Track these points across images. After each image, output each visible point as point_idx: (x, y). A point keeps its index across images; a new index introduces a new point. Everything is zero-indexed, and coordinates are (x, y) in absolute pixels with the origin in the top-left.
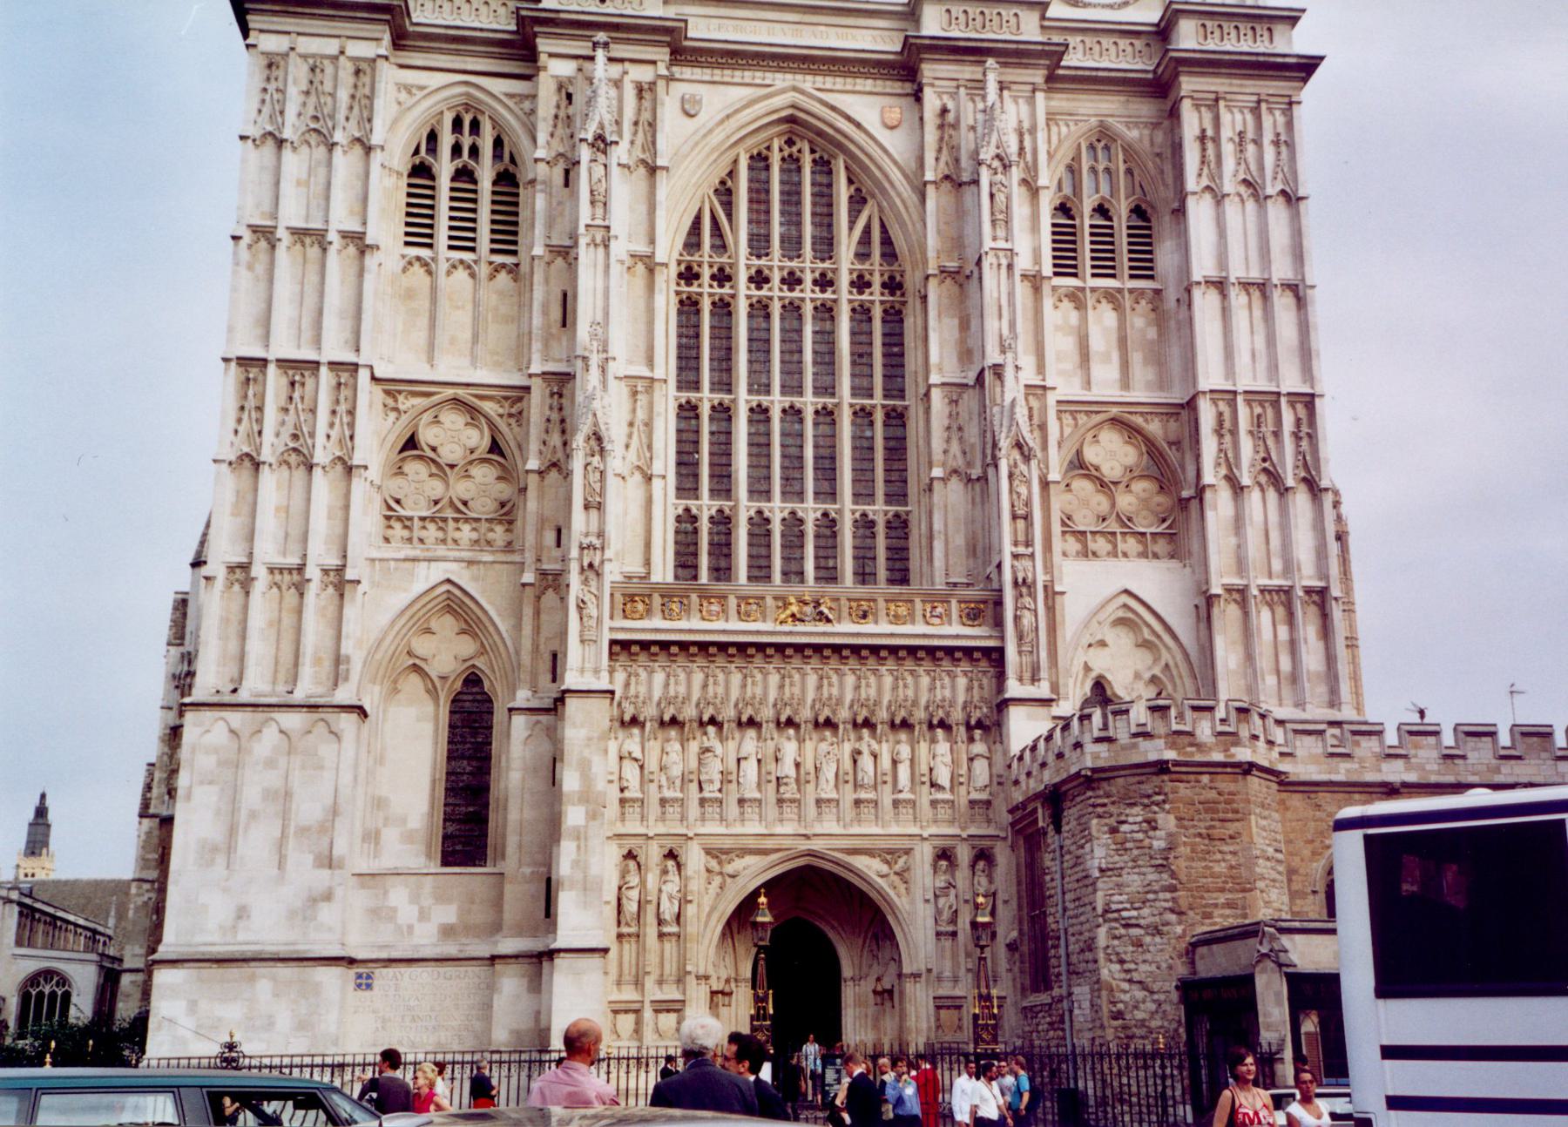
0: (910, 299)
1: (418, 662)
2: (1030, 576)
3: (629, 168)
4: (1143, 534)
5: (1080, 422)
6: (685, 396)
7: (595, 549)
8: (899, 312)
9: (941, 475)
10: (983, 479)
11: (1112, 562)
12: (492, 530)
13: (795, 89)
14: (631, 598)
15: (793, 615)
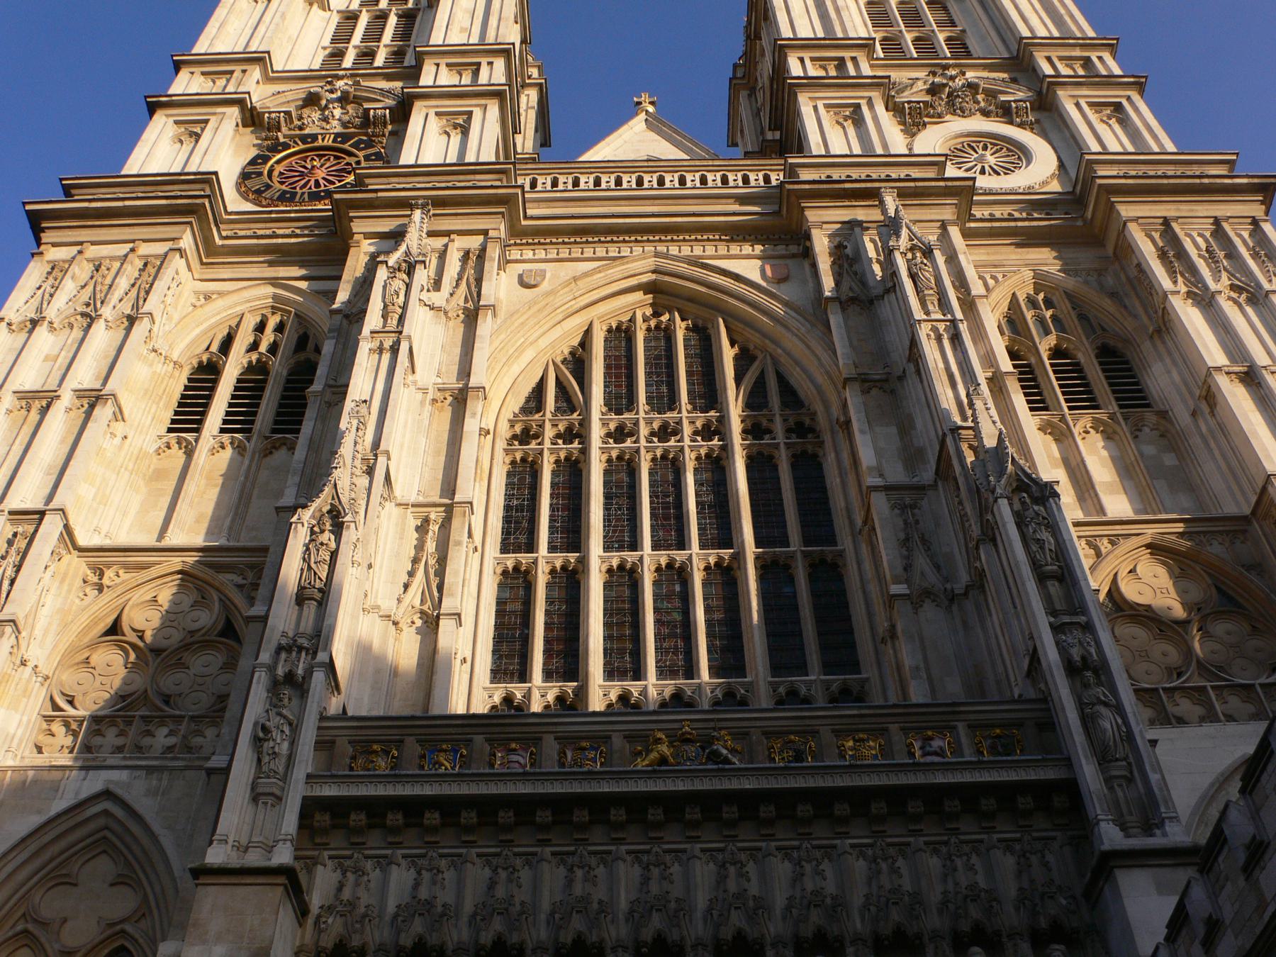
0: (827, 437)
1: (30, 927)
2: (1093, 651)
3: (446, 313)
4: (1249, 688)
5: (1104, 551)
6: (510, 561)
7: (300, 649)
8: (815, 456)
9: (908, 592)
10: (979, 582)
11: (1209, 729)
12: (200, 733)
13: (657, 255)
14: (364, 748)
15: (663, 761)
